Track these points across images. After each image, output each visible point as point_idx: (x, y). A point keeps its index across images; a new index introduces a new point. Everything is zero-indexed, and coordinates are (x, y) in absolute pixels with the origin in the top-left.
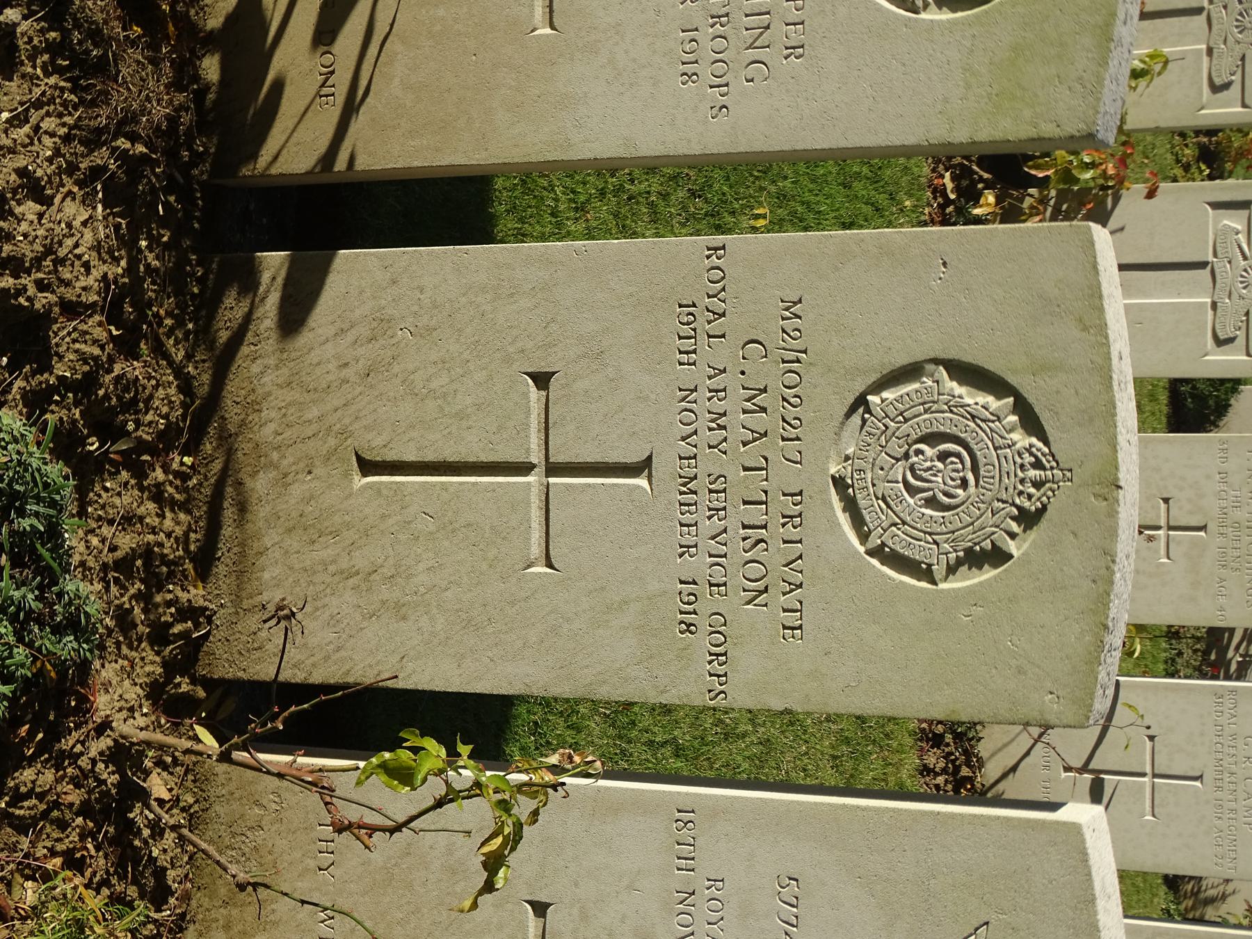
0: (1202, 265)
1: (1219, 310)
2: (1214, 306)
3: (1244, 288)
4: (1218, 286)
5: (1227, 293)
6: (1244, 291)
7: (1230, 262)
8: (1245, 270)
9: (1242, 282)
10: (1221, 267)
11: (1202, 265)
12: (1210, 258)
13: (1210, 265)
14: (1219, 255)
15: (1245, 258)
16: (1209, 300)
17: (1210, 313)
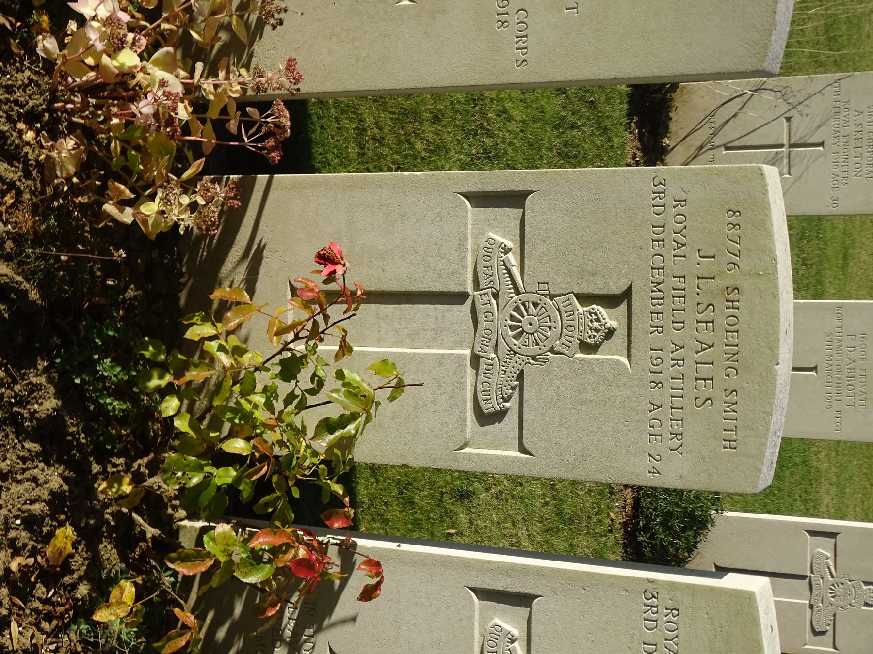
0: (803, 577)
1: (815, 609)
2: (811, 606)
3: (833, 597)
4: (813, 594)
6: (833, 599)
7: (822, 578)
8: (833, 585)
9: (831, 593)
10: (817, 581)
11: (803, 577)
12: (809, 574)
13: (808, 578)
15: (832, 577)
16: (807, 602)
17: (808, 610)
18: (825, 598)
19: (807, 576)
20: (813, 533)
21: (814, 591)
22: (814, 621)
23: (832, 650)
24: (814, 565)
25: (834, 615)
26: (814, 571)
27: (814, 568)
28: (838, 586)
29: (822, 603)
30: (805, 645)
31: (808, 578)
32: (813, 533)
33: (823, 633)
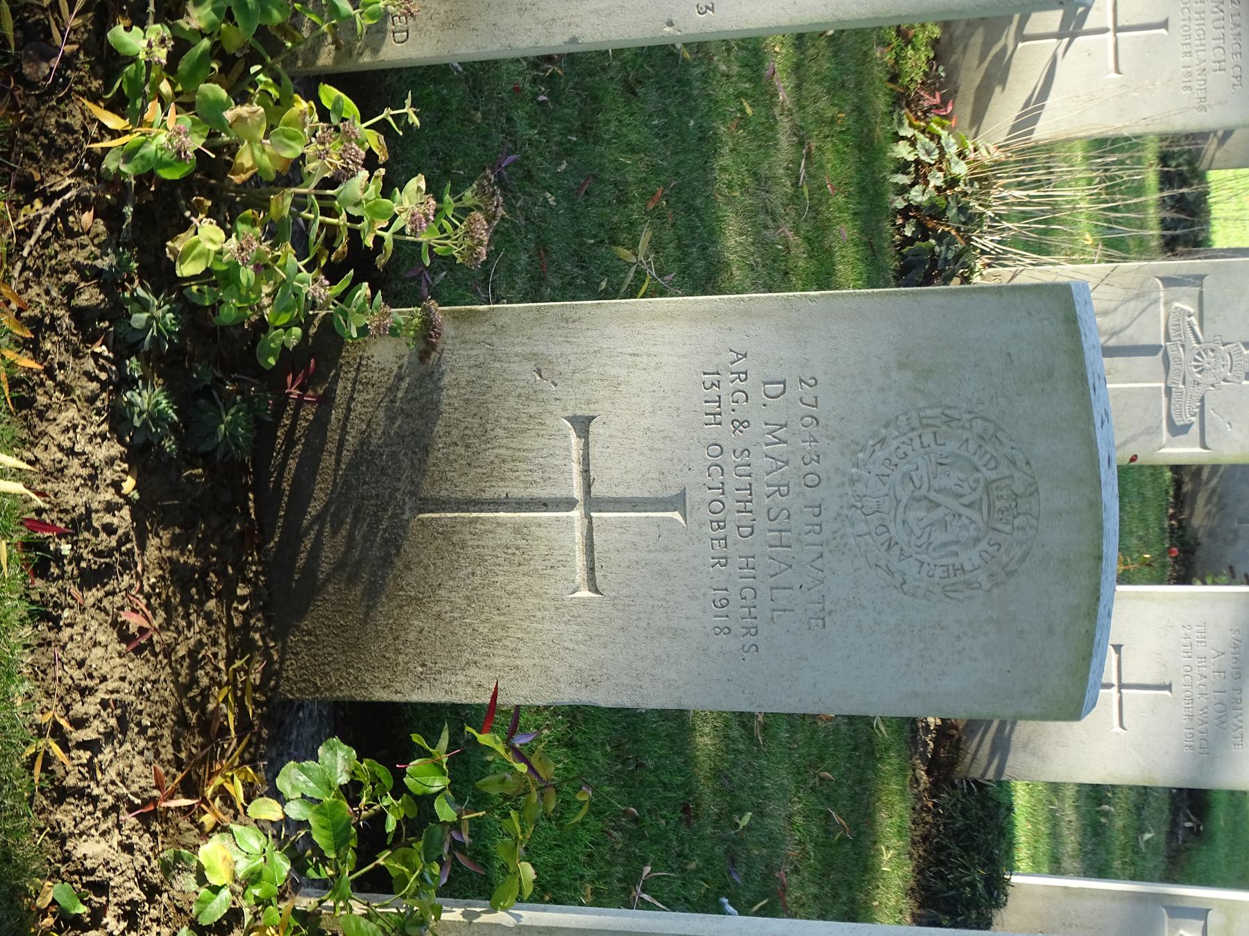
1: (1174, 395)
2: (1168, 391)
3: (1200, 372)
5: (1181, 378)
6: (1199, 376)
7: (1183, 346)
8: (1199, 354)
9: (1196, 367)
12: (1163, 344)
14: (1173, 339)
15: (1198, 342)
16: (1162, 385)
18: (1188, 376)
19: (1161, 346)
20: (1169, 282)
21: (1172, 368)
23: (1199, 450)
24: (1171, 327)
25: (1202, 400)
28: (1206, 354)
29: (1184, 383)
32: (1169, 282)
33: (1185, 429)
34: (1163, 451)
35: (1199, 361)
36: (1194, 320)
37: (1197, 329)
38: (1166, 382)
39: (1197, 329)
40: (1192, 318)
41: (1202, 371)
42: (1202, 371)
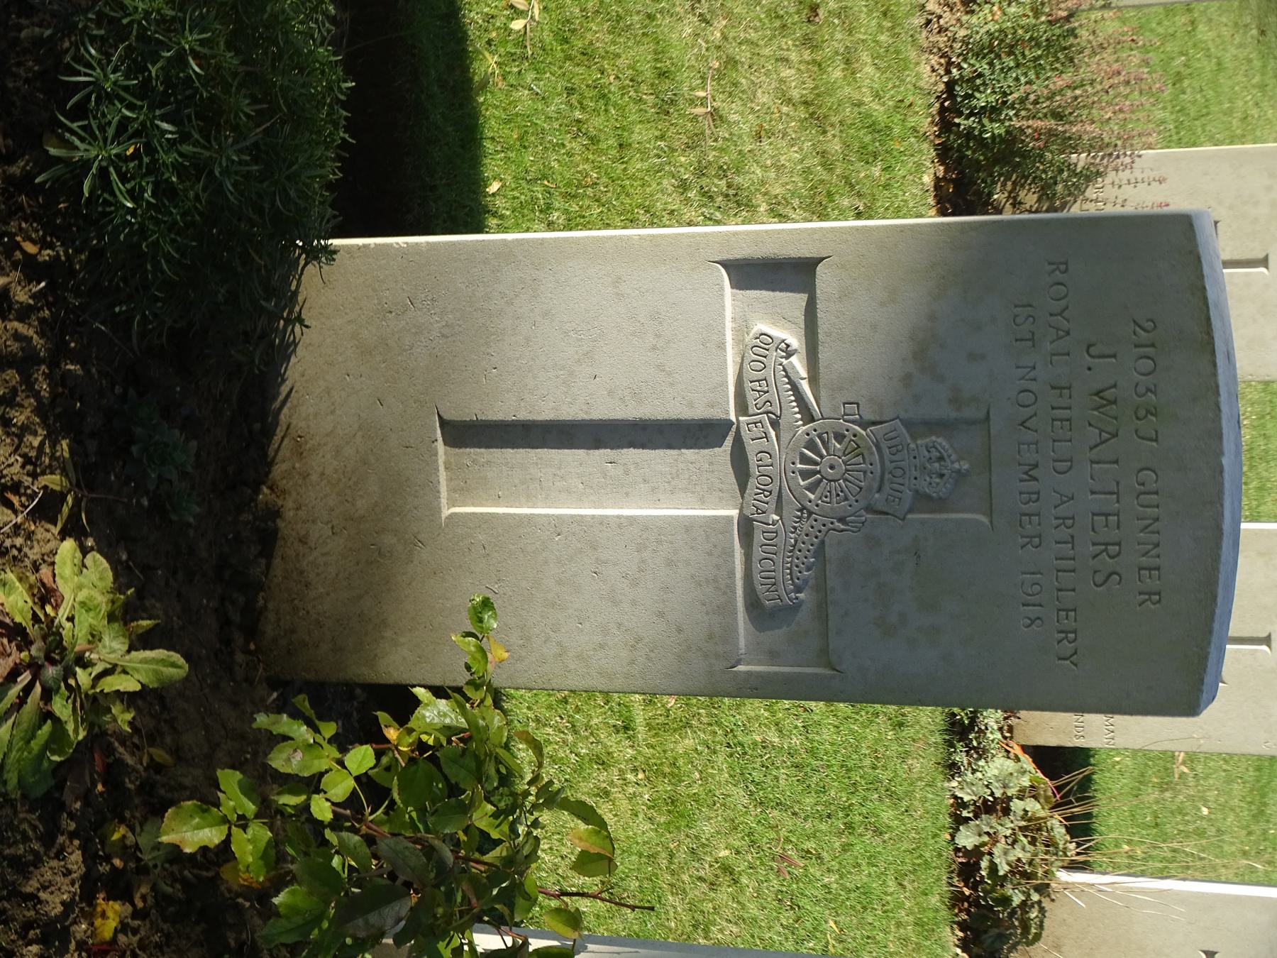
1: (759, 538)
2: (746, 526)
3: (811, 488)
6: (812, 497)
7: (775, 424)
8: (811, 446)
9: (805, 475)
12: (733, 418)
13: (735, 426)
14: (752, 410)
15: (809, 417)
16: (734, 513)
22: (757, 578)
24: (748, 385)
26: (751, 403)
27: (751, 396)
29: (779, 511)
30: (738, 662)
31: (735, 426)
34: (741, 668)
35: (816, 463)
36: (798, 364)
37: (805, 386)
38: (741, 510)
39: (805, 386)
40: (794, 359)
41: (820, 481)
42: (820, 481)
